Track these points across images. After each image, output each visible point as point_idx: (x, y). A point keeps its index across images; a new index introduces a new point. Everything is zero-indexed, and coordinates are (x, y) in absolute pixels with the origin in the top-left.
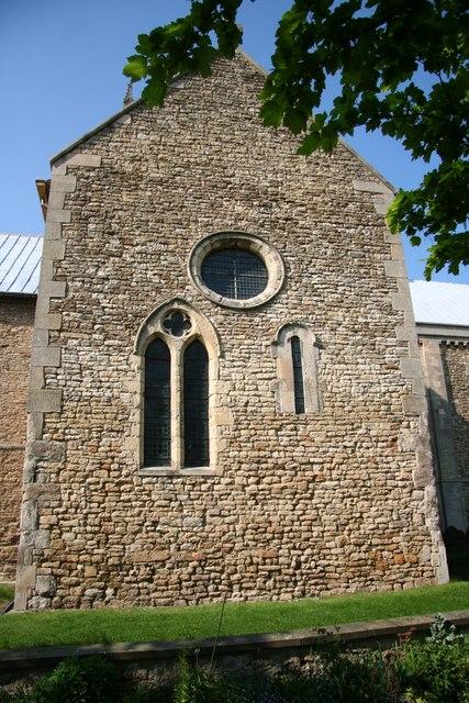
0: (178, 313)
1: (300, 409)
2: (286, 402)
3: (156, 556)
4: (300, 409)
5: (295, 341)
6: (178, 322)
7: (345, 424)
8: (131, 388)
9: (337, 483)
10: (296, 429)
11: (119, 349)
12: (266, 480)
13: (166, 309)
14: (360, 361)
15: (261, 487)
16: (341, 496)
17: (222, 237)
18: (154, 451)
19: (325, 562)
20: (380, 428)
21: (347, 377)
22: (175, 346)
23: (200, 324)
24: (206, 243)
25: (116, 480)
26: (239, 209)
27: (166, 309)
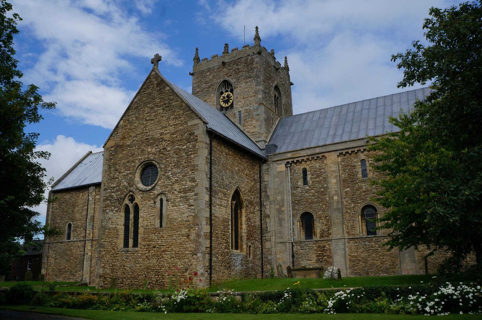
0: (132, 196)
1: (161, 226)
2: (157, 224)
3: (124, 276)
4: (161, 226)
5: (161, 200)
6: (132, 199)
7: (174, 230)
8: (122, 221)
9: (170, 252)
10: (159, 233)
11: (116, 211)
12: (151, 252)
13: (128, 195)
14: (181, 204)
15: (149, 254)
16: (170, 257)
17: (144, 163)
18: (126, 245)
19: (164, 281)
20: (185, 231)
21: (176, 212)
22: (131, 205)
23: (138, 200)
24: (140, 167)
25: (116, 253)
26: (149, 150)
27: (128, 195)
